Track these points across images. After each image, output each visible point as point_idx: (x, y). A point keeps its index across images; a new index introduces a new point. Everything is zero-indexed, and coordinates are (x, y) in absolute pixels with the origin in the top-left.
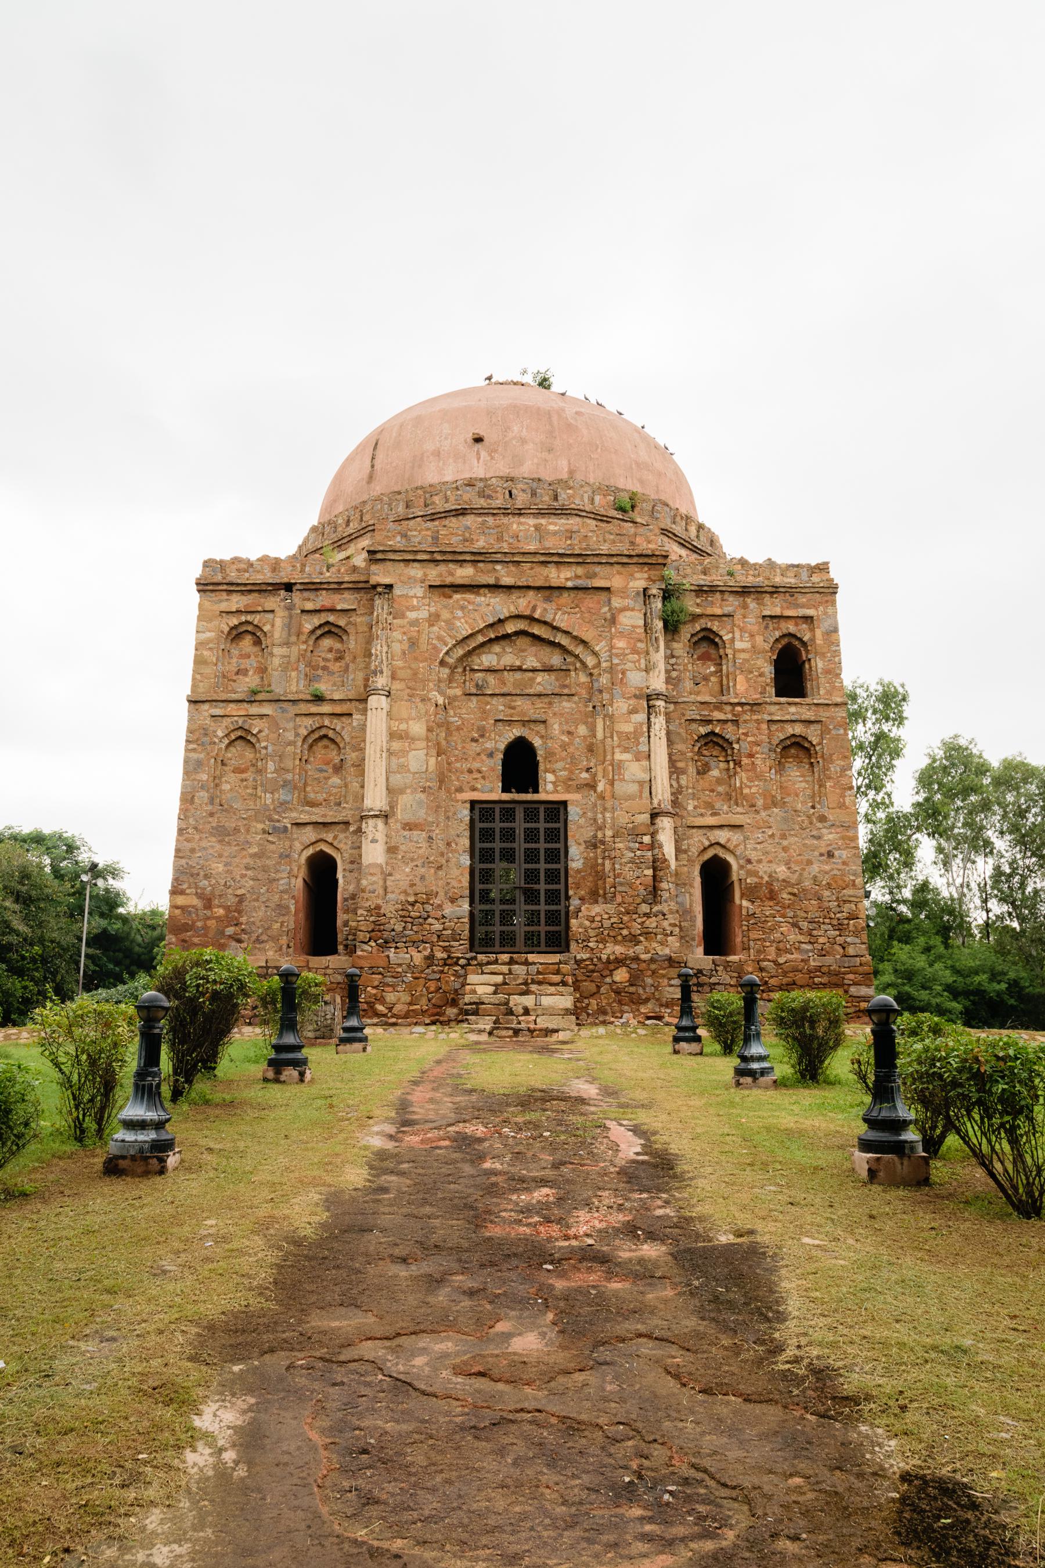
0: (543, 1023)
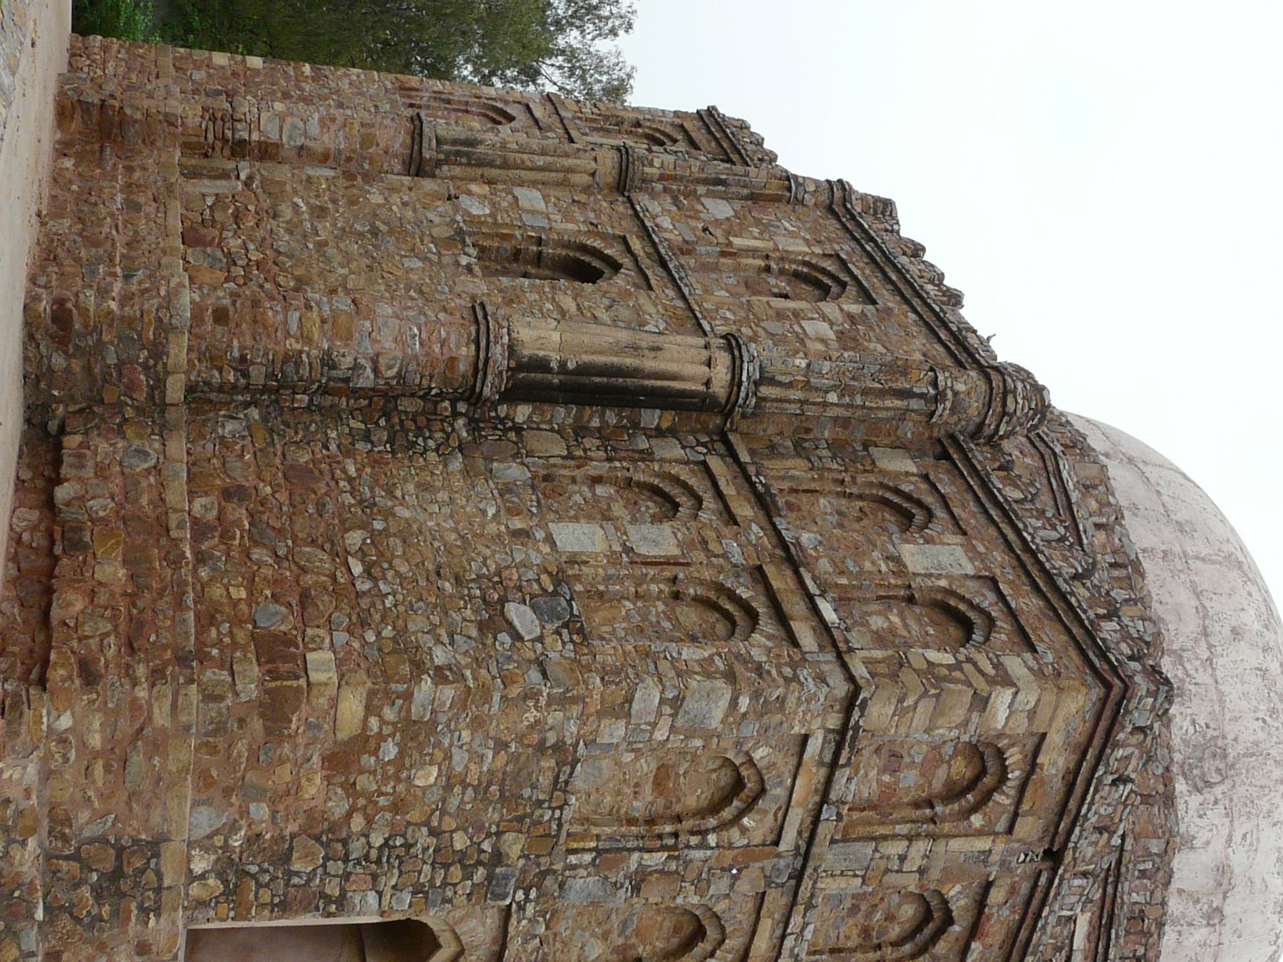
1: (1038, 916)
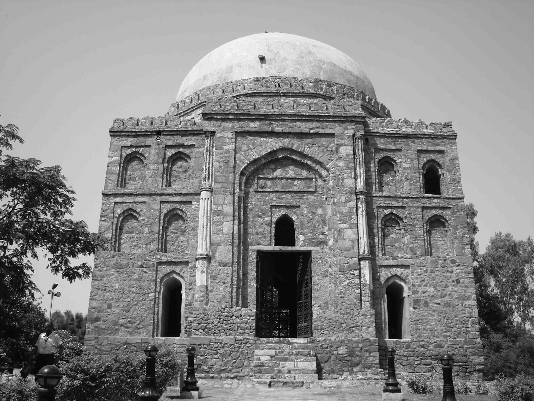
0: (299, 378)
1: (176, 131)
